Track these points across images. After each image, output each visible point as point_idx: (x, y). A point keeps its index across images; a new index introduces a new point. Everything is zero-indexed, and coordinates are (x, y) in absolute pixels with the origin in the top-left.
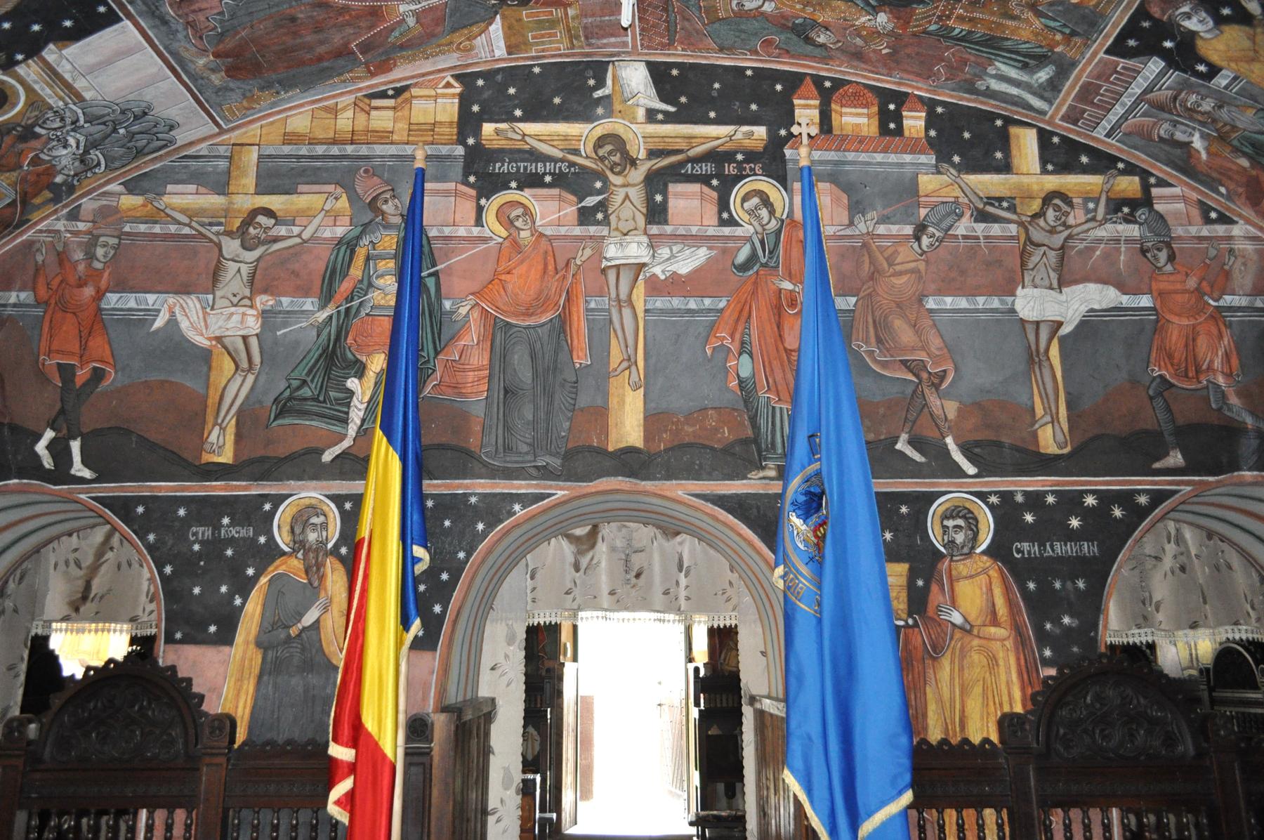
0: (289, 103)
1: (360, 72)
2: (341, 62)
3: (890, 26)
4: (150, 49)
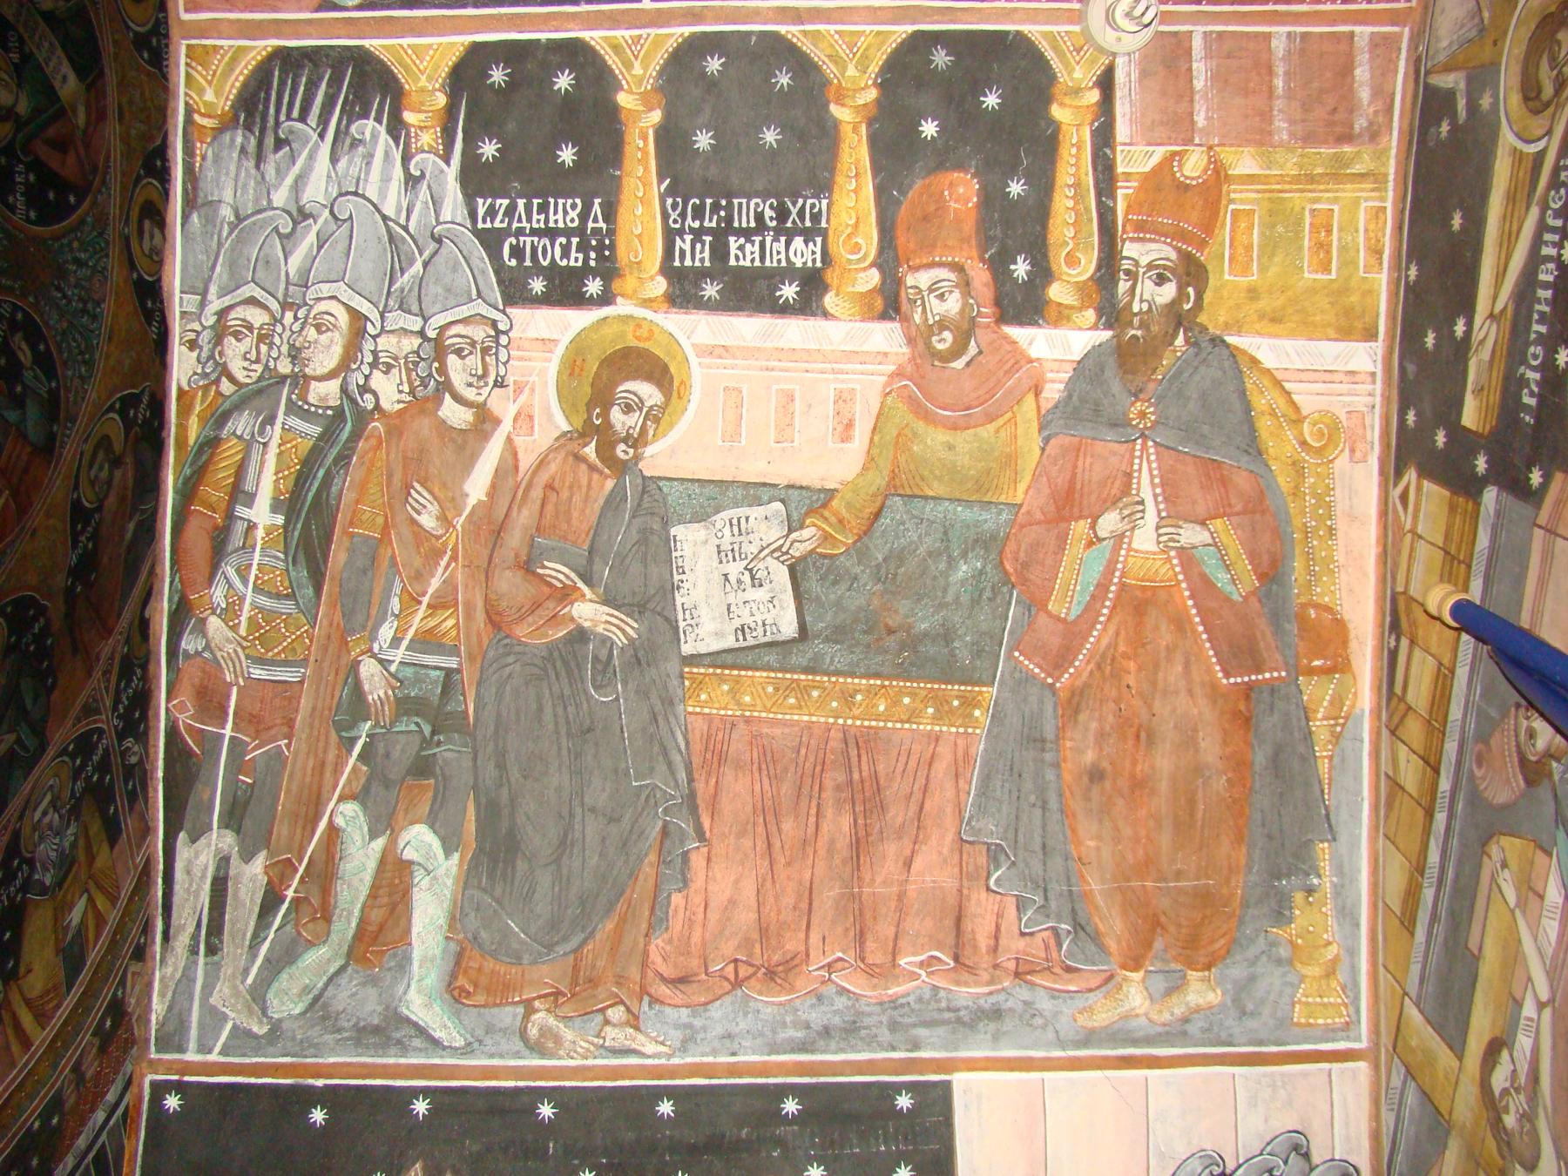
0: (1354, 880)
1: (1317, 693)
2: (1269, 723)
4: (1047, 1075)
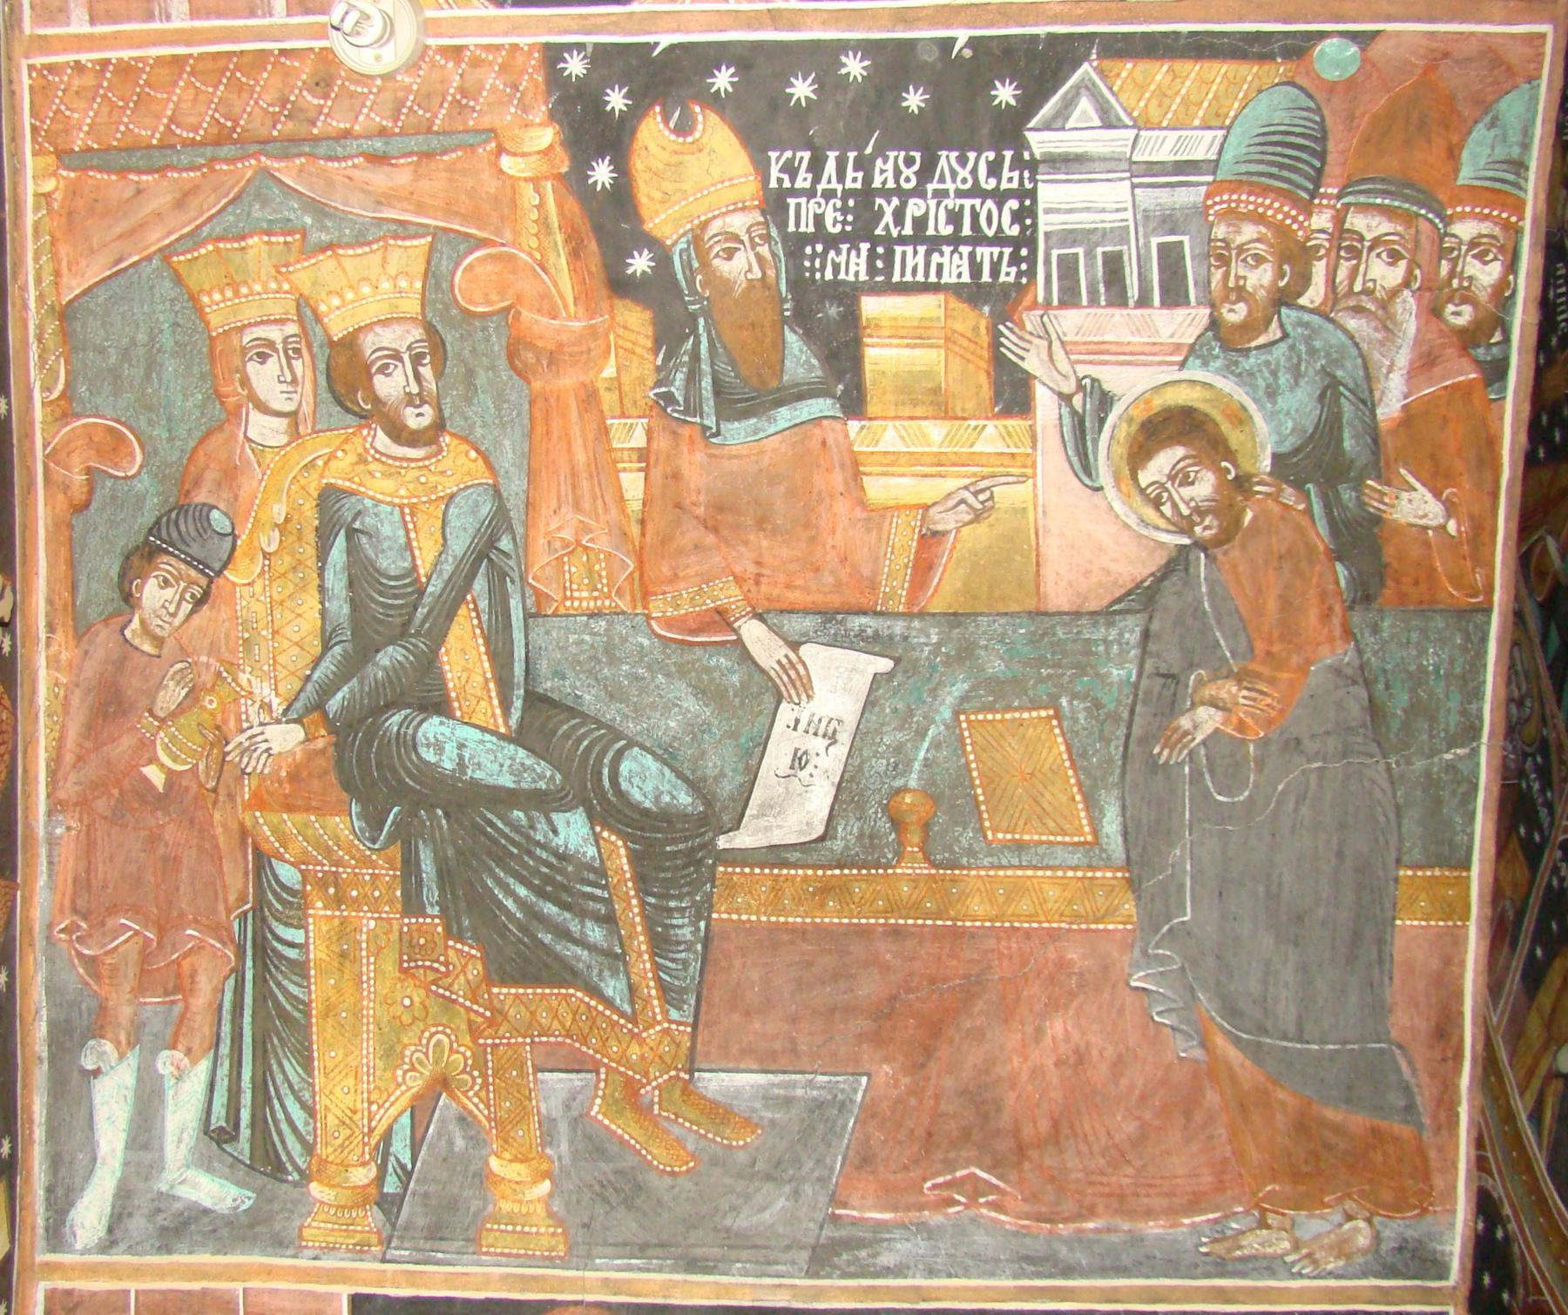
3: (257, 764)
